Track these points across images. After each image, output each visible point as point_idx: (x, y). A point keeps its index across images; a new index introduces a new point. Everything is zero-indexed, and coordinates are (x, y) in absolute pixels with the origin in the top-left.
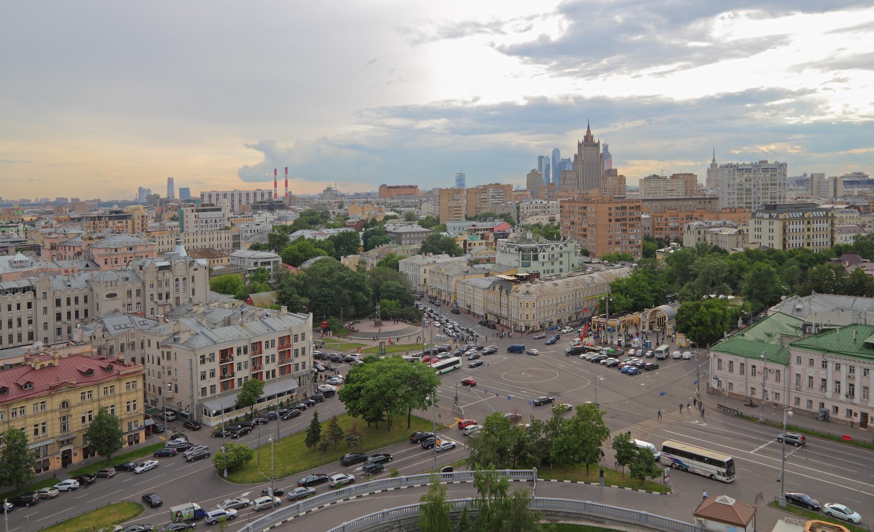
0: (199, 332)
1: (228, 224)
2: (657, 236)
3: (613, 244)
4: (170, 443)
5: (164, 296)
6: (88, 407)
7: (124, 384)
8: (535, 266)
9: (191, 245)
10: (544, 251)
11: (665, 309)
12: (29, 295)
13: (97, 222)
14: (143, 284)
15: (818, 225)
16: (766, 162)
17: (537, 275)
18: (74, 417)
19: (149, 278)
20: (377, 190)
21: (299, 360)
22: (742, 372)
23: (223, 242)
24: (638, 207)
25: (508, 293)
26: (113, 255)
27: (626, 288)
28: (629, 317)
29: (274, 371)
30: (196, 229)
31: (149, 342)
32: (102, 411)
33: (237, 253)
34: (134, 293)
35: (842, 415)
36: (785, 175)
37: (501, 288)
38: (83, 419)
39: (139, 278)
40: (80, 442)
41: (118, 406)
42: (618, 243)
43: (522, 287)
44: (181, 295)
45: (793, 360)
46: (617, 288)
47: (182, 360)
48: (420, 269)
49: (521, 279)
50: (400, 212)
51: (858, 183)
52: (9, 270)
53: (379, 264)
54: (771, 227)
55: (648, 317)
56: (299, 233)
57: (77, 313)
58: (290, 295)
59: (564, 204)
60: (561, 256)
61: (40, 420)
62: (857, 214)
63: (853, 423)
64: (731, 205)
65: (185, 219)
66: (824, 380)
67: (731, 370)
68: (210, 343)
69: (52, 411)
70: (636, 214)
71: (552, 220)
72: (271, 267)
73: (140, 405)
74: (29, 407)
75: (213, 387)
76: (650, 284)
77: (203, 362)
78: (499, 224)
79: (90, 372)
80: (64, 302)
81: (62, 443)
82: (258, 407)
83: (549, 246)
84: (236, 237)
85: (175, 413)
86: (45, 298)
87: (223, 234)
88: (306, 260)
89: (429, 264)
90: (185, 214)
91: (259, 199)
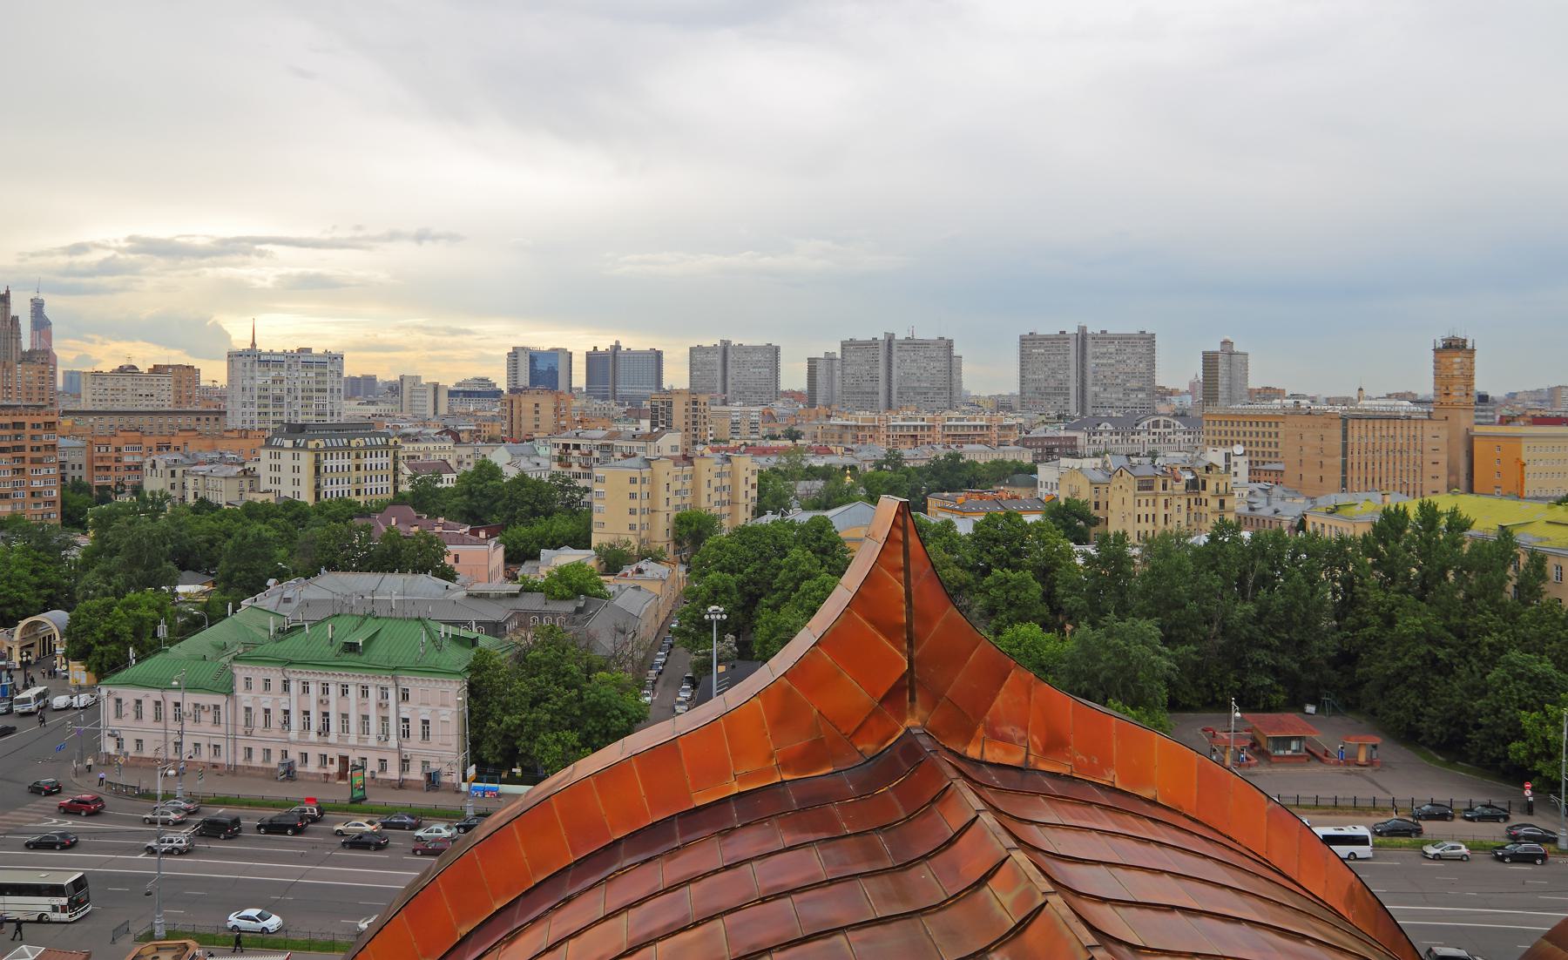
2: (97, 482)
11: (55, 619)
15: (374, 461)
16: (309, 350)
22: (158, 718)
24: (50, 425)
35: (313, 767)
36: (340, 375)
45: (240, 684)
51: (478, 394)
54: (296, 463)
55: (17, 637)
62: (449, 443)
63: (327, 775)
64: (247, 426)
66: (287, 712)
67: (139, 716)
70: (46, 438)
76: (34, 572)
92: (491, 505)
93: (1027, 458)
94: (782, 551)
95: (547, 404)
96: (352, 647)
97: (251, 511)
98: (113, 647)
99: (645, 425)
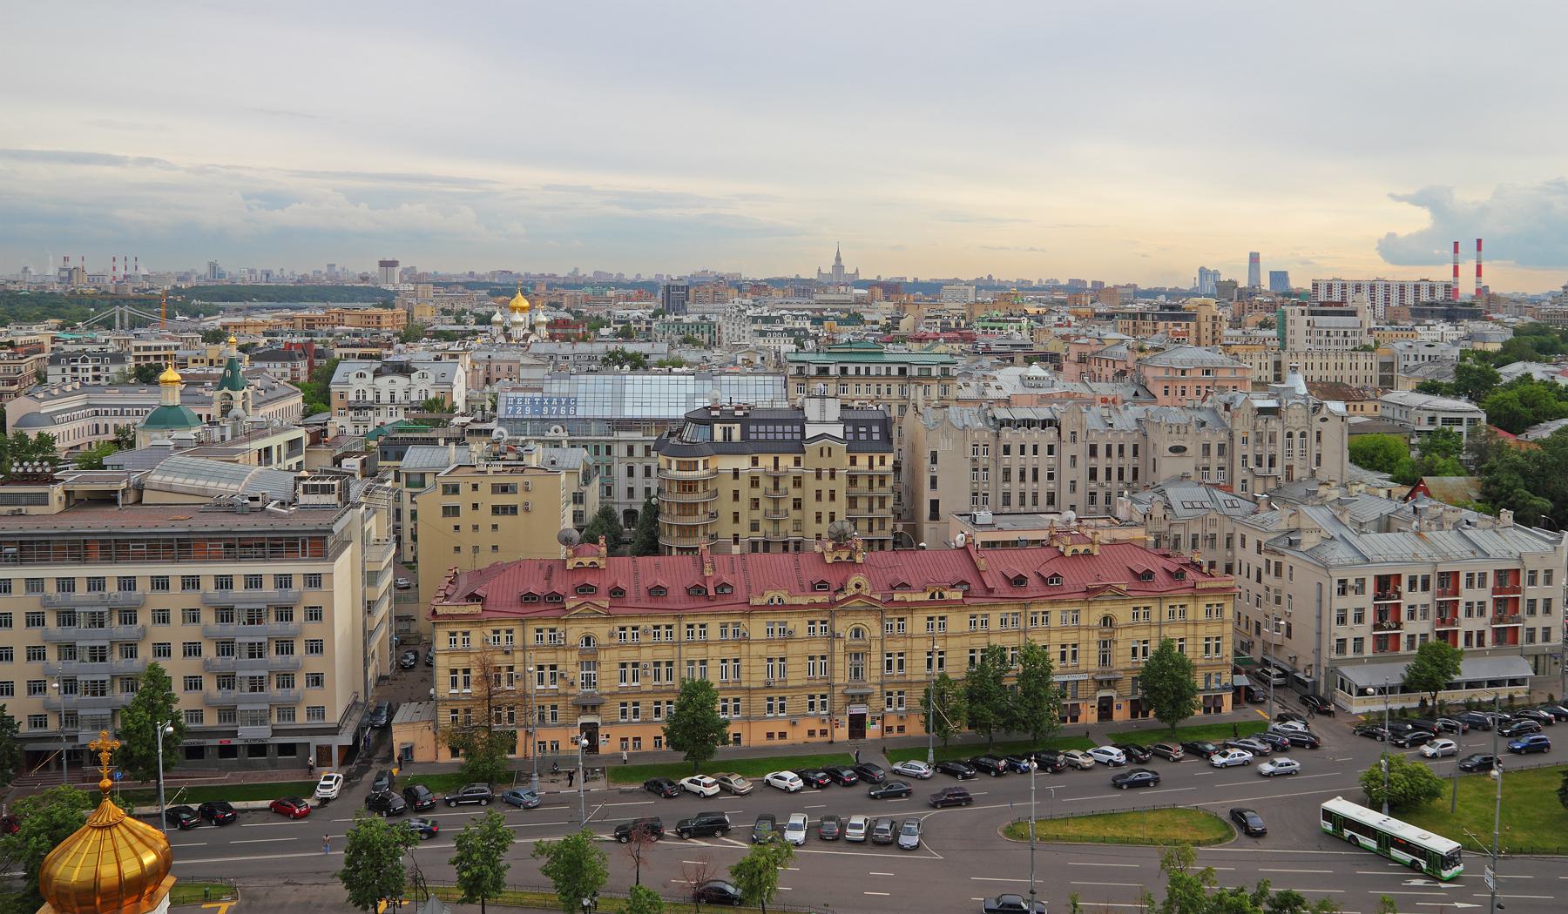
0: (1337, 536)
1: (1369, 341)
4: (1277, 726)
5: (1266, 462)
6: (1142, 634)
7: (1202, 607)
9: (1316, 374)
12: (1051, 433)
13: (1139, 322)
14: (1231, 435)
18: (1120, 645)
19: (1241, 427)
21: (1538, 622)
23: (1361, 373)
26: (1178, 380)
29: (1481, 634)
30: (1308, 346)
31: (1243, 539)
32: (1166, 646)
33: (1393, 396)
34: (1214, 450)
38: (1134, 650)
39: (1224, 424)
40: (1126, 687)
41: (1190, 641)
44: (1297, 463)
47: (1302, 581)
52: (1020, 390)
56: (1515, 369)
57: (1121, 471)
58: (1510, 489)
61: (1070, 638)
65: (1289, 327)
68: (1357, 560)
69: (1088, 628)
72: (1464, 429)
73: (1228, 649)
74: (1056, 614)
75: (1359, 642)
77: (1342, 591)
79: (1148, 575)
80: (1101, 451)
81: (1100, 684)
82: (1443, 695)
84: (1387, 366)
85: (1285, 674)
86: (1074, 440)
87: (1362, 359)
88: (1537, 423)
90: (1289, 317)
91: (1425, 297)
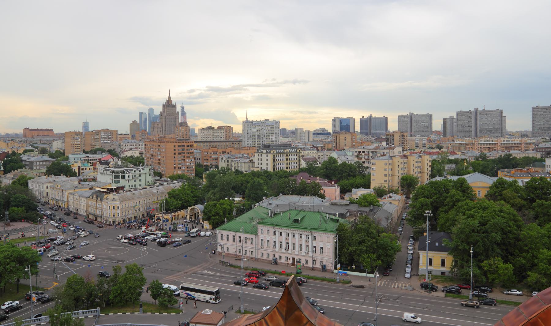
2: (205, 164)
3: (177, 168)
8: (122, 183)
10: (129, 173)
11: (199, 208)
15: (292, 157)
16: (268, 120)
17: (122, 188)
20: (22, 132)
22: (234, 241)
24: (192, 146)
25: (101, 200)
27: (177, 195)
28: (178, 213)
35: (283, 260)
36: (278, 128)
37: (97, 197)
42: (179, 168)
43: (111, 196)
45: (260, 232)
46: (173, 195)
48: (42, 186)
49: (110, 191)
50: (37, 148)
51: (322, 134)
53: (14, 183)
54: (267, 158)
55: (189, 212)
59: (147, 143)
60: (140, 176)
62: (315, 151)
63: (288, 264)
64: (249, 146)
66: (275, 242)
67: (228, 240)
71: (141, 153)
76: (192, 192)
78: (105, 156)
83: (132, 170)
89: (50, 182)
92: (334, 172)
93: (538, 156)
94: (447, 191)
95: (349, 137)
96: (296, 221)
97: (254, 174)
98: (217, 217)
99: (384, 144)
